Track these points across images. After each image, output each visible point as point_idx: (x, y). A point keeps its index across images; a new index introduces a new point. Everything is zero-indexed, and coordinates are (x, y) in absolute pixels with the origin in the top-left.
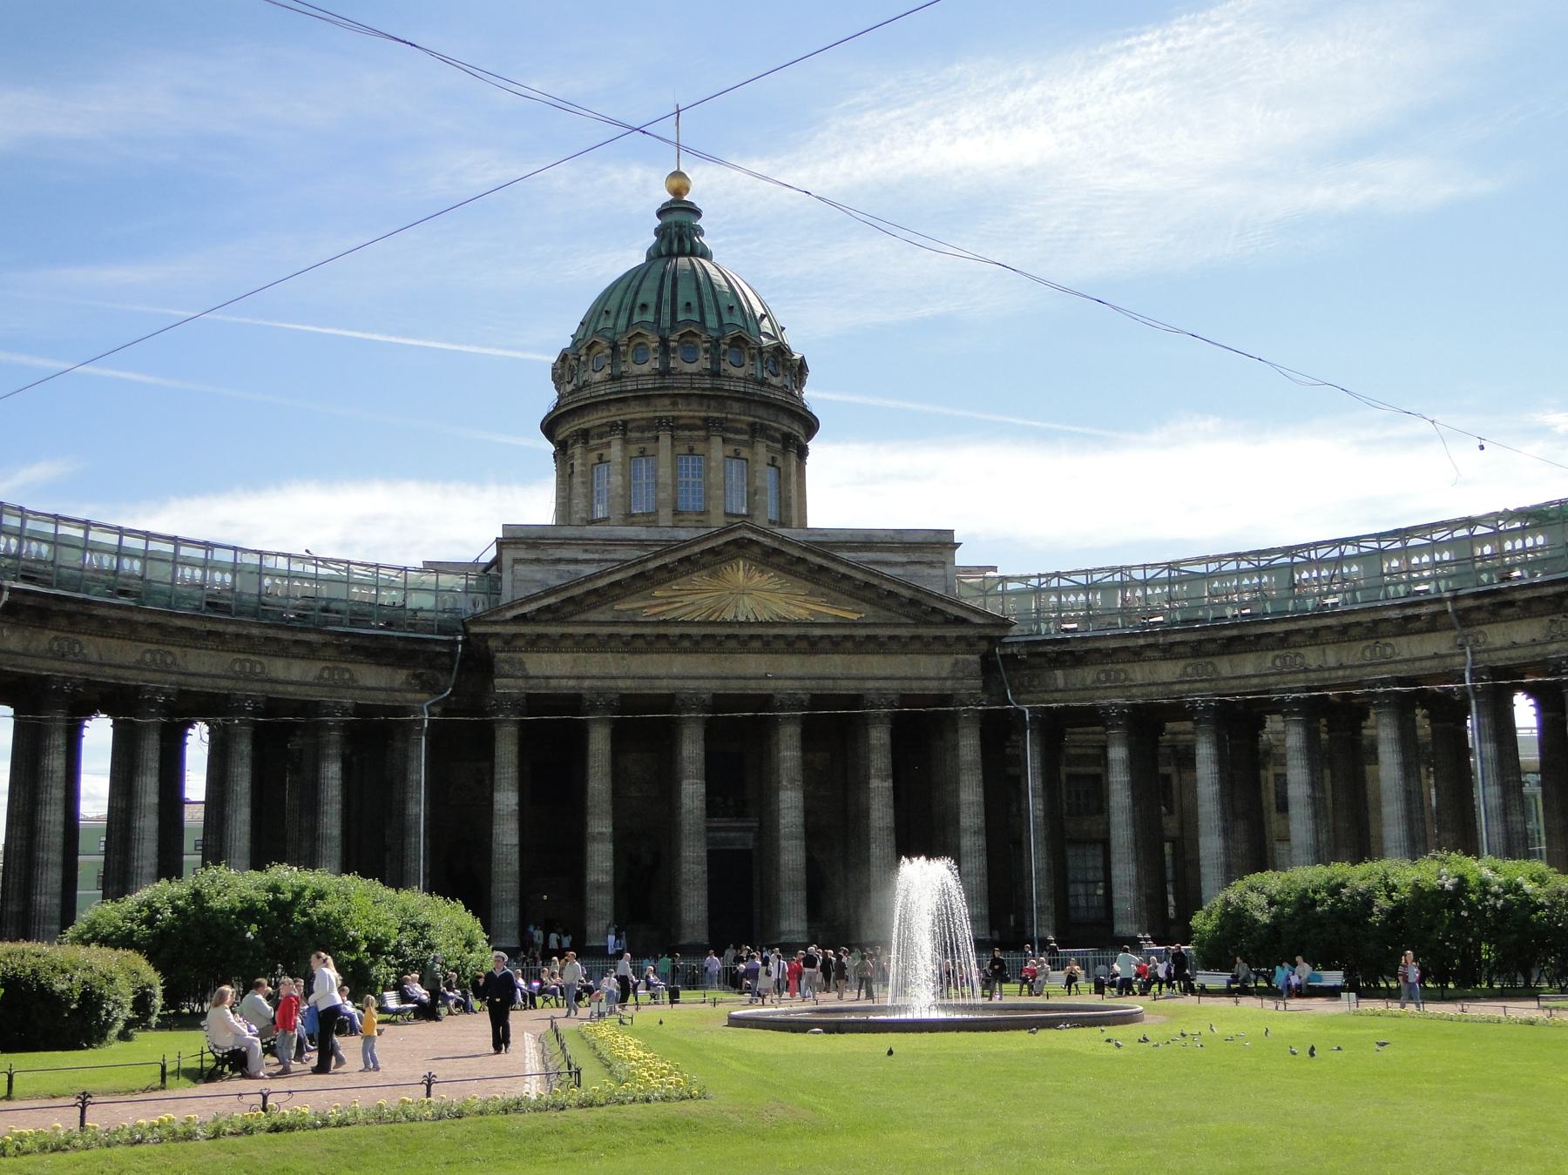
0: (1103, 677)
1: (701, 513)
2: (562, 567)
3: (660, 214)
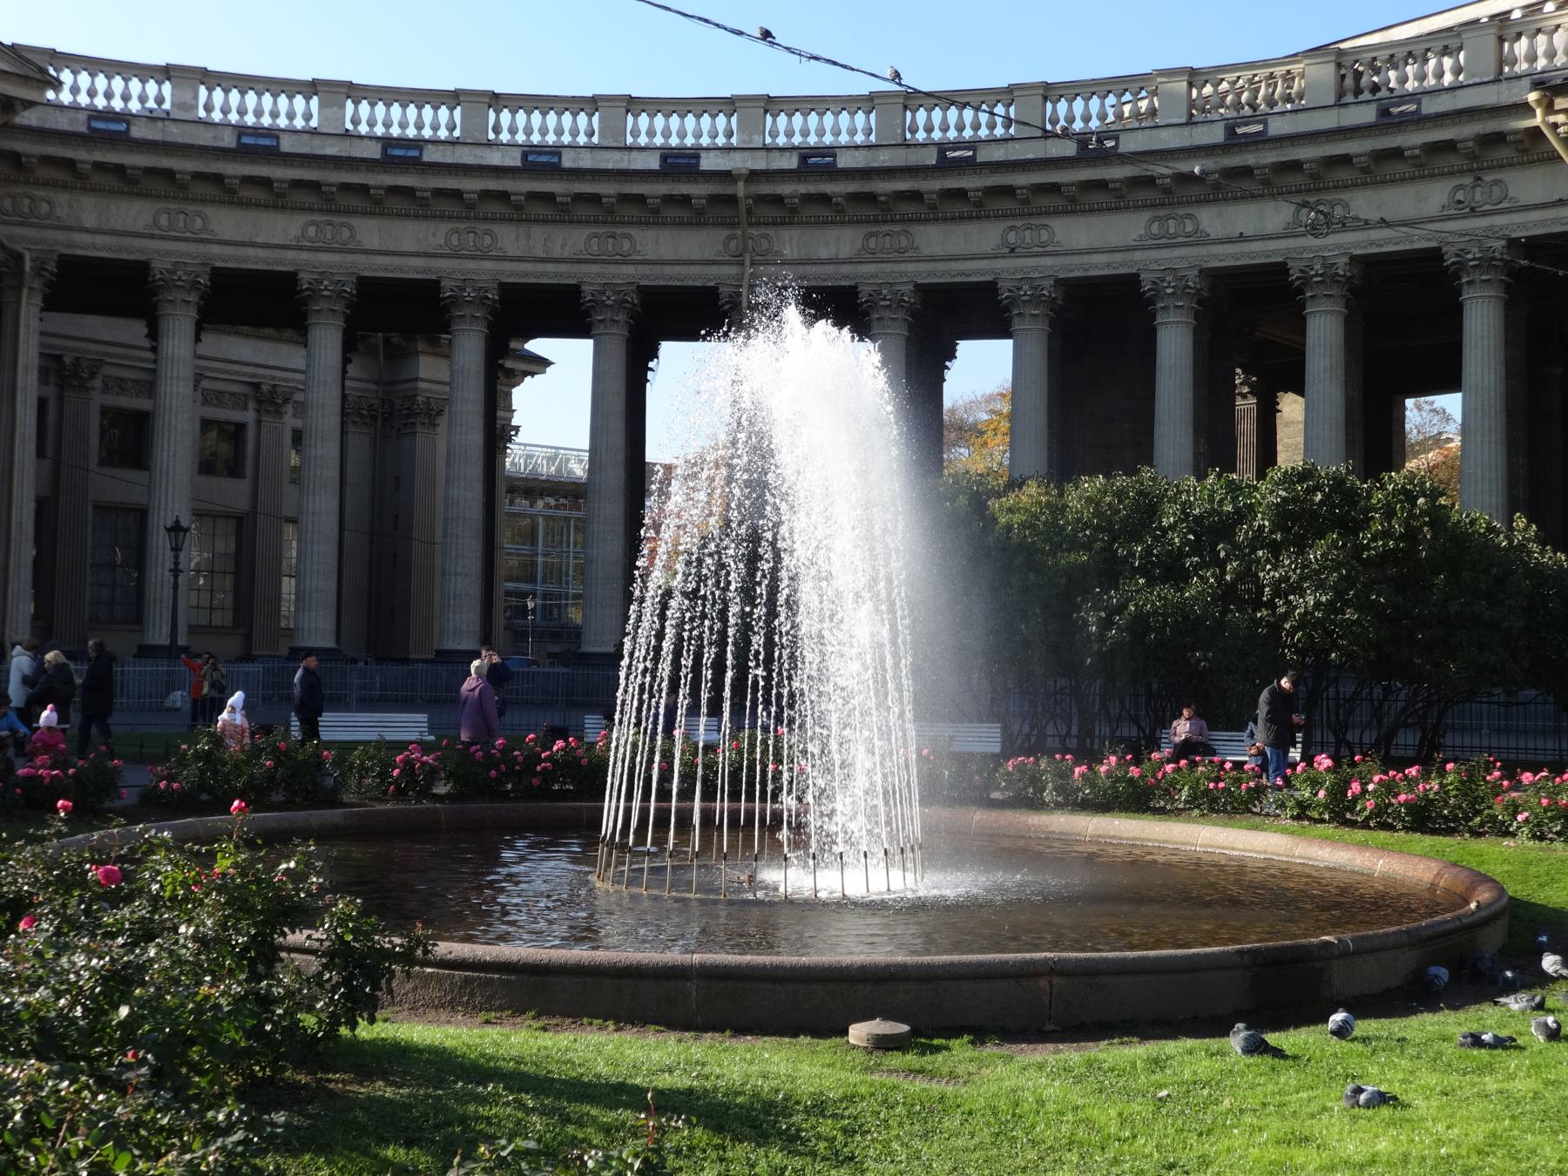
0: (164, 220)
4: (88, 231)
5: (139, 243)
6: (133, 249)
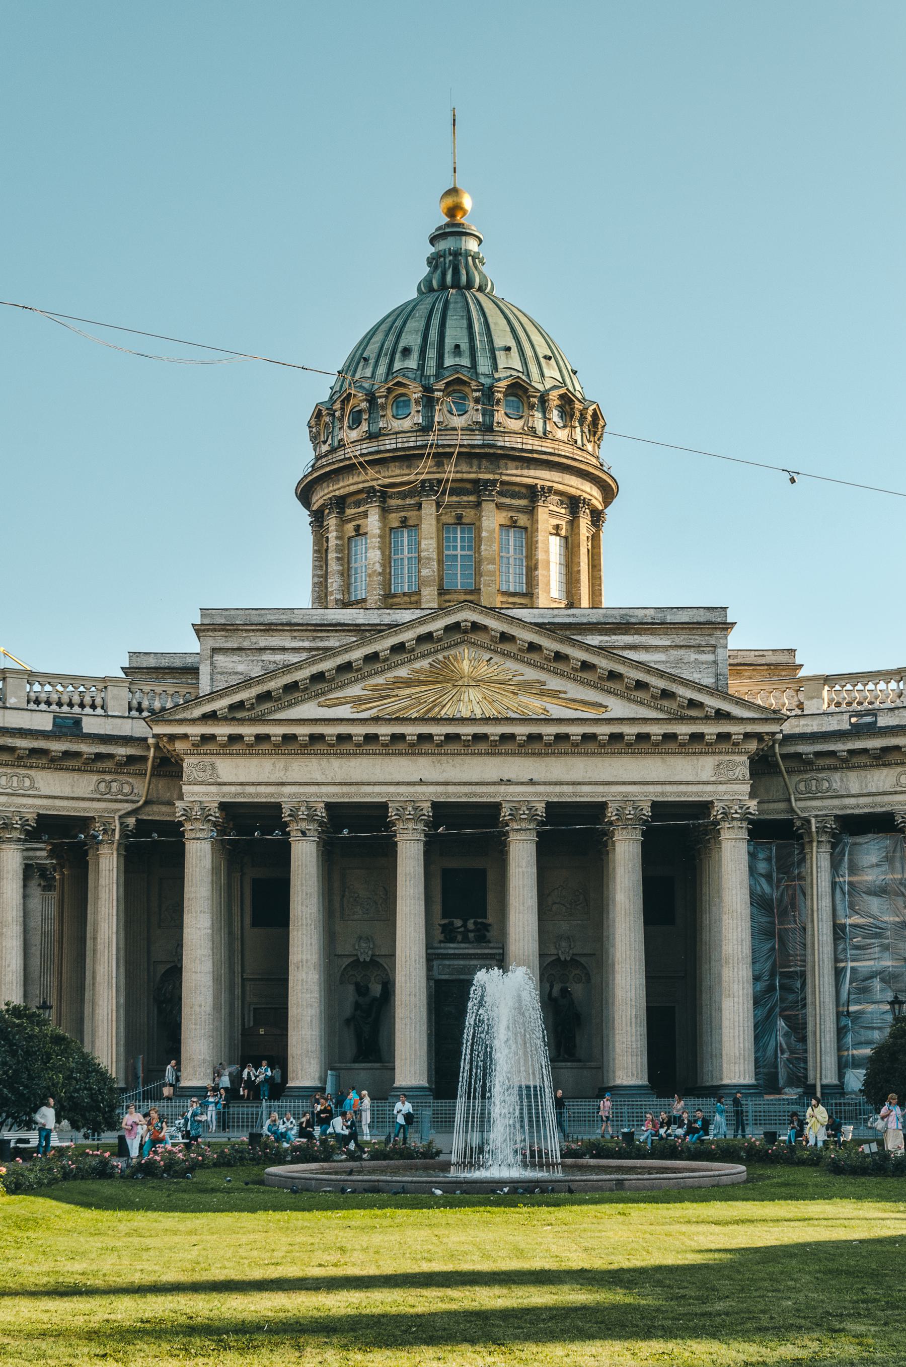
1: (471, 592)
2: (267, 657)
3: (433, 240)
4: (853, 796)
5: (886, 799)
6: (882, 804)
